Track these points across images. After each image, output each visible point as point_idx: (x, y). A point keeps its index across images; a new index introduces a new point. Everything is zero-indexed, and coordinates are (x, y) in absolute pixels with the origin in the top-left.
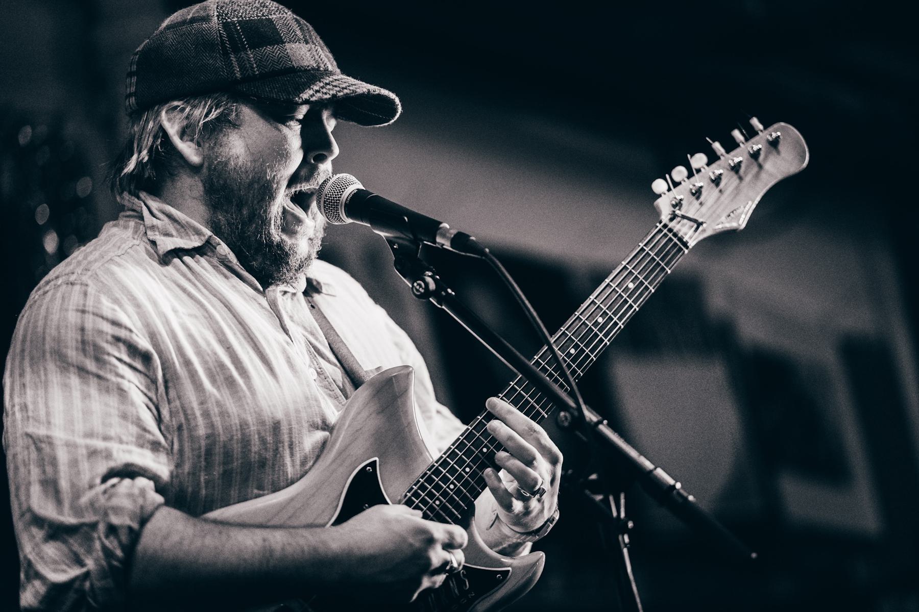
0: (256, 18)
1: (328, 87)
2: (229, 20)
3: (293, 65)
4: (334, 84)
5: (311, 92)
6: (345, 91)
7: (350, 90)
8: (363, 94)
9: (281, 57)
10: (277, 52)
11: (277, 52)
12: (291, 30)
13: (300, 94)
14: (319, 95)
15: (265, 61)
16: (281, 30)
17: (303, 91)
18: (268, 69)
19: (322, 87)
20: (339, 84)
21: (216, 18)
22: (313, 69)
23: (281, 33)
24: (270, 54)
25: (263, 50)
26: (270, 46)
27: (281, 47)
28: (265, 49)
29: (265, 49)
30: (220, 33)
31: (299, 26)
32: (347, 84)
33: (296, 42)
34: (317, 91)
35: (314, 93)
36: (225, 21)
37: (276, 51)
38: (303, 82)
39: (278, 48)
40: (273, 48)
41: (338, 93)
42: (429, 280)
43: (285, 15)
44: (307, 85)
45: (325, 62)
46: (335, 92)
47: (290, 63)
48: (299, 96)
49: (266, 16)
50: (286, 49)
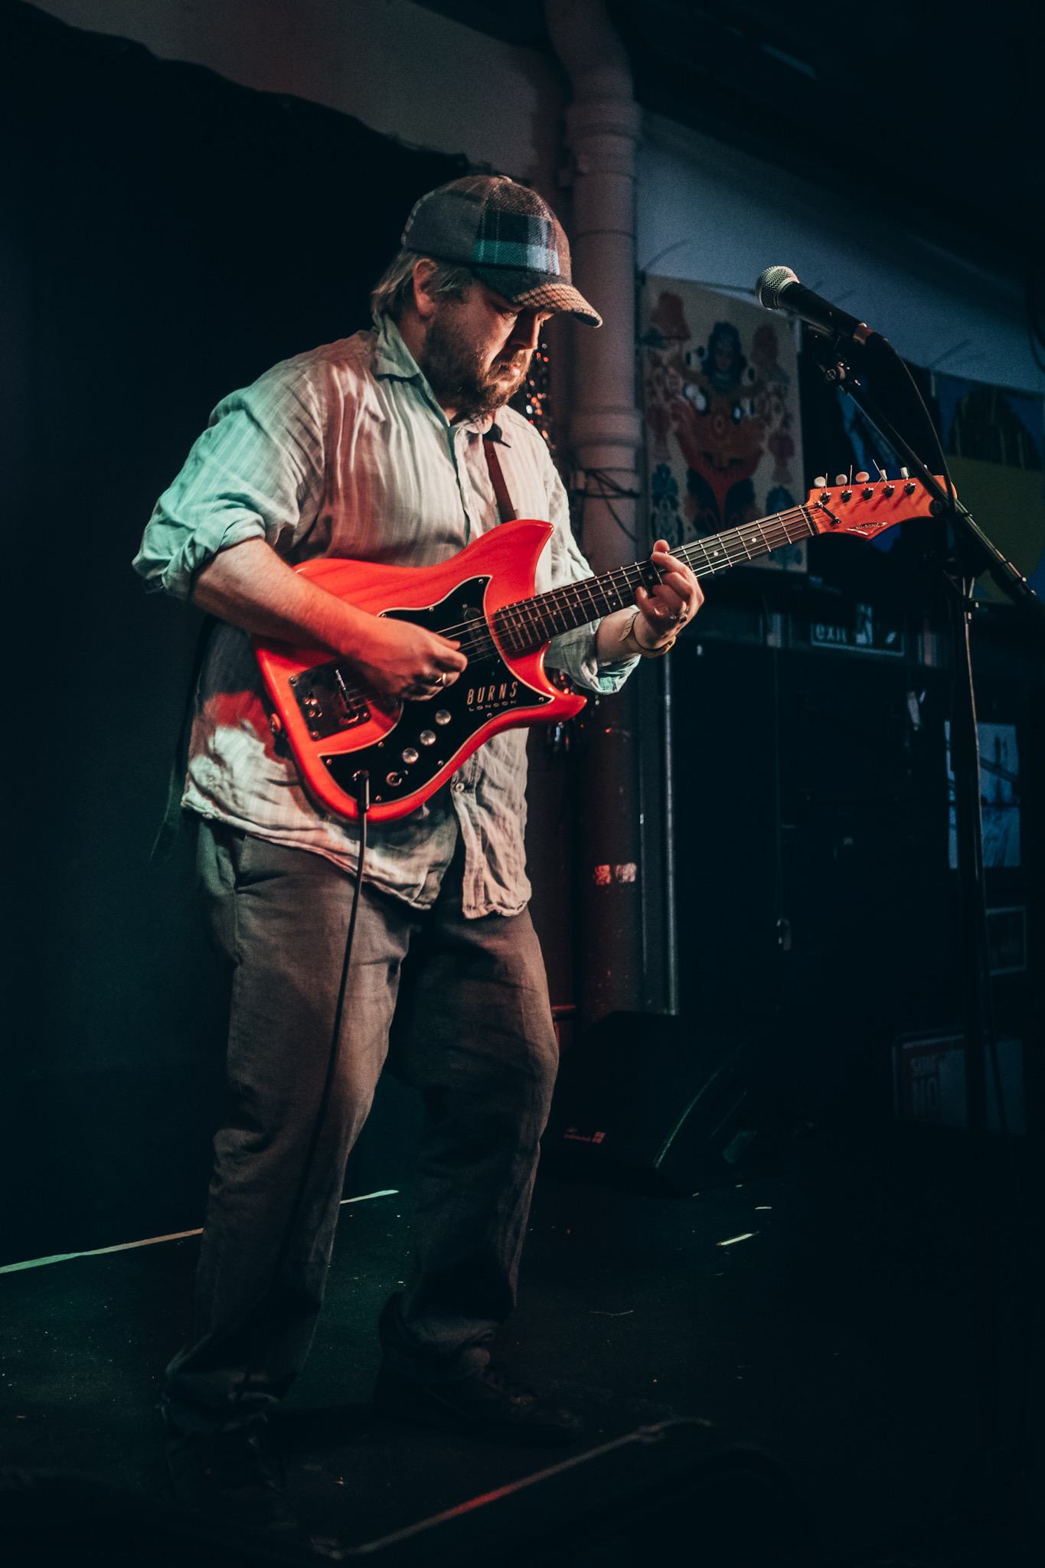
1: (543, 296)
5: (527, 296)
8: (567, 311)
14: (532, 301)
17: (521, 292)
19: (538, 295)
22: (543, 273)
34: (532, 297)
42: (842, 370)
44: (528, 289)
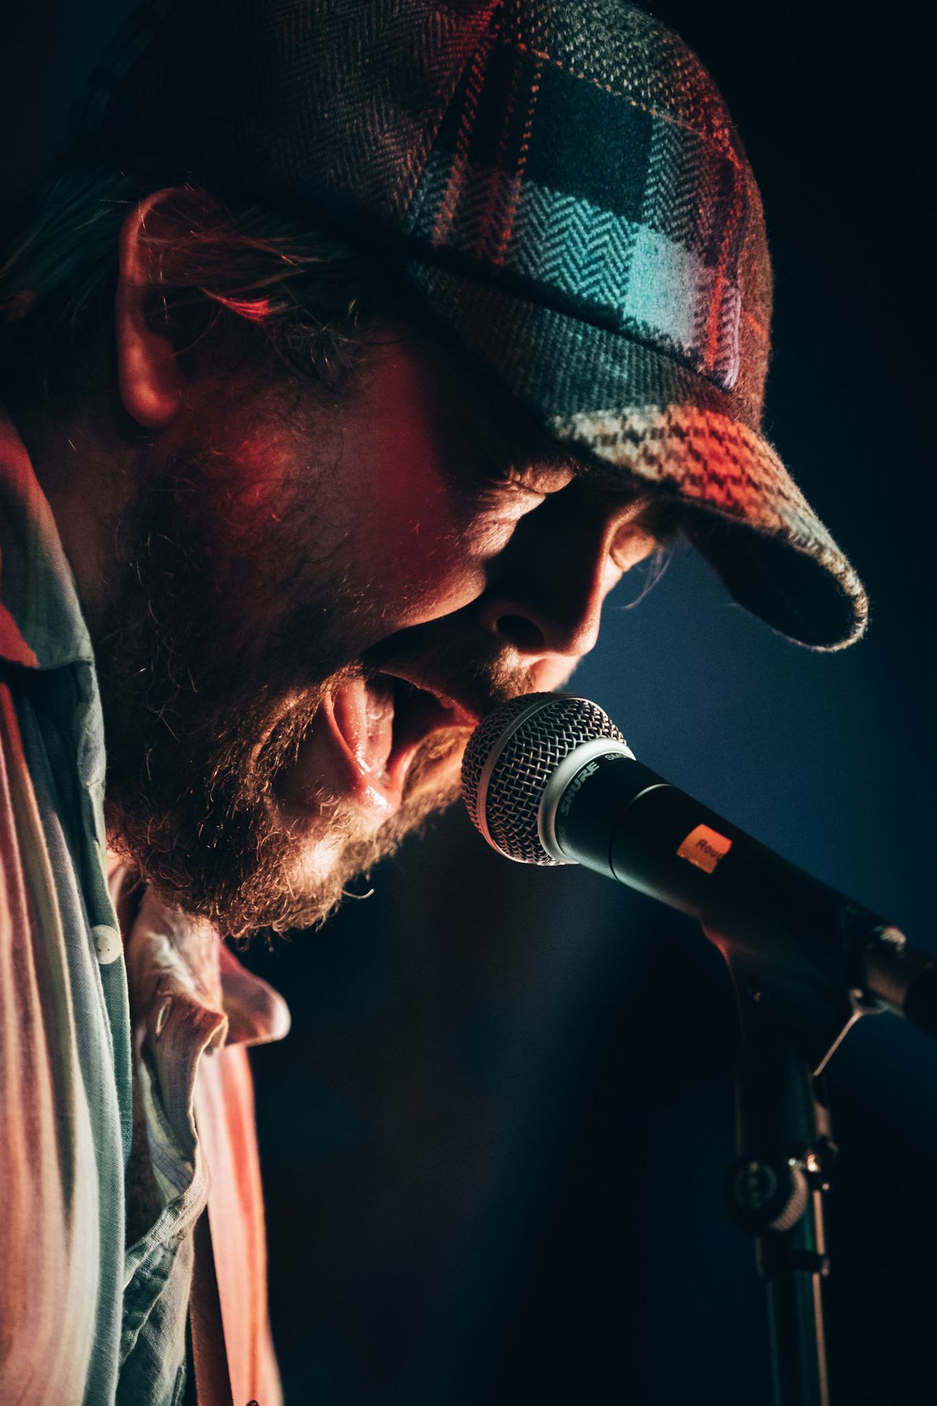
0: (609, 88)
2: (523, 46)
3: (623, 305)
4: (699, 444)
6: (714, 491)
7: (729, 495)
10: (599, 236)
11: (599, 236)
13: (579, 410)
15: (547, 239)
16: (655, 173)
18: (542, 270)
20: (714, 455)
21: (487, 16)
23: (651, 185)
24: (574, 225)
25: (564, 202)
26: (591, 205)
27: (623, 227)
28: (569, 204)
29: (569, 204)
30: (468, 71)
31: (719, 194)
32: (736, 471)
33: (677, 240)
34: (633, 437)
35: (621, 433)
36: (508, 41)
37: (599, 230)
38: (612, 378)
39: (609, 226)
40: (596, 214)
41: (687, 482)
43: (702, 135)
45: (728, 353)
46: (681, 472)
47: (617, 291)
48: (570, 414)
49: (646, 100)
50: (632, 243)
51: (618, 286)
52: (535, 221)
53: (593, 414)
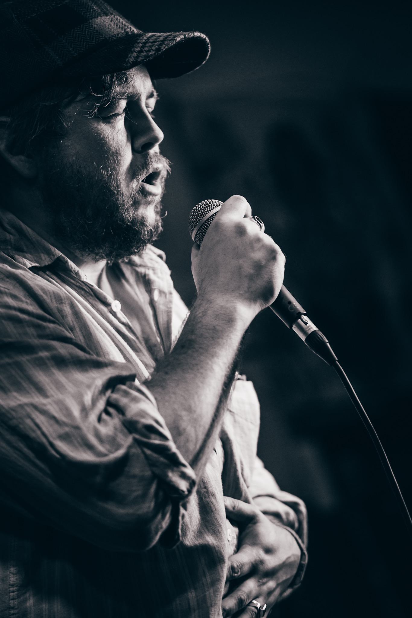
1: (148, 45)
9: (91, 33)
11: (85, 31)
12: (88, 7)
18: (84, 48)
34: (140, 52)
37: (84, 30)
39: (84, 27)
51: (100, 35)
52: (72, 41)
53: (128, 57)
